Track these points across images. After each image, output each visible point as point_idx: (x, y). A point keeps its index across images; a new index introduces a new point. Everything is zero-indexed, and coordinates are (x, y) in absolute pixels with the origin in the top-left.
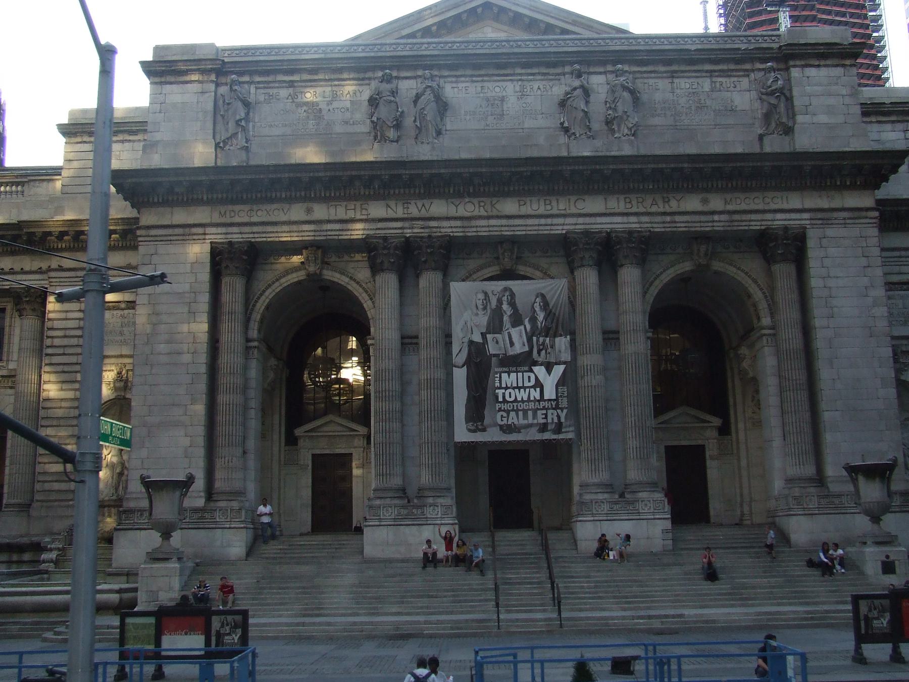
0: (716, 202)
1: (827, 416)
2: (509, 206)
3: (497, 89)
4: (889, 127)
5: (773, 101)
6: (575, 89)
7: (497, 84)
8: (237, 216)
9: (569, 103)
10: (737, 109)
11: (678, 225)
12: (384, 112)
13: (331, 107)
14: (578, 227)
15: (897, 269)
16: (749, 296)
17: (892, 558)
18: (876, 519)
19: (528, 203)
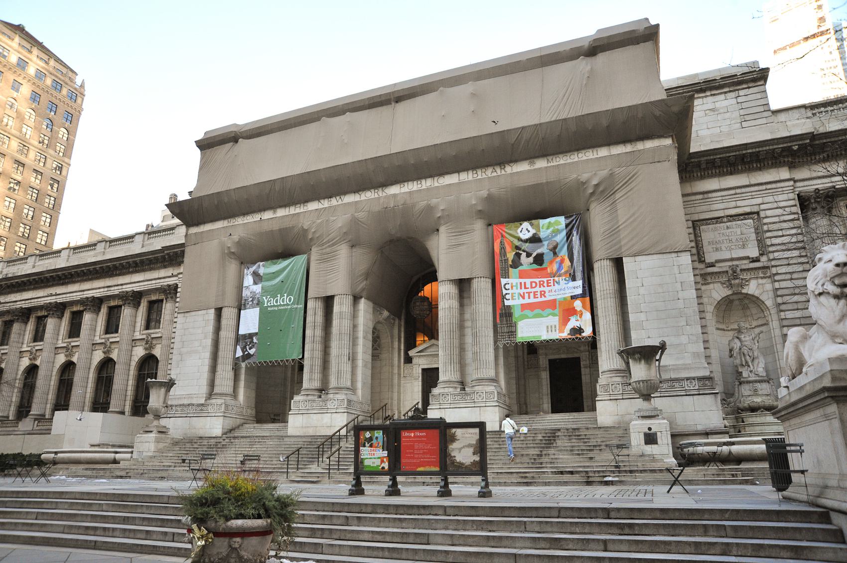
1: (632, 317)
4: (722, 97)
15: (733, 204)
17: (653, 431)
18: (647, 397)
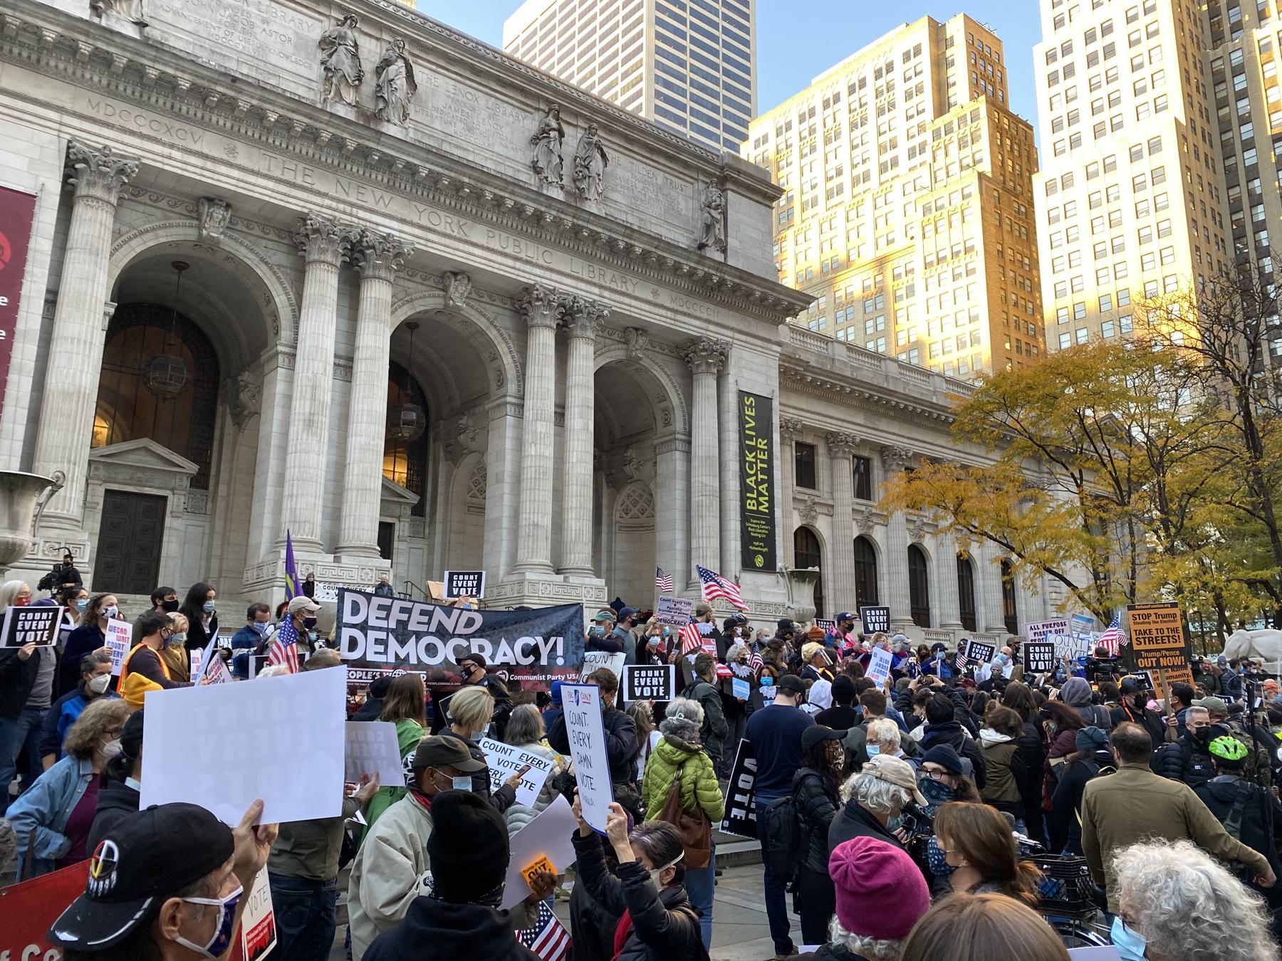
0: (665, 298)
2: (479, 234)
3: (469, 96)
5: (715, 214)
6: (554, 129)
7: (473, 91)
8: (117, 115)
9: (544, 142)
10: (683, 213)
11: (633, 309)
12: (342, 59)
13: (265, 26)
14: (544, 281)
16: (664, 398)
19: (497, 237)
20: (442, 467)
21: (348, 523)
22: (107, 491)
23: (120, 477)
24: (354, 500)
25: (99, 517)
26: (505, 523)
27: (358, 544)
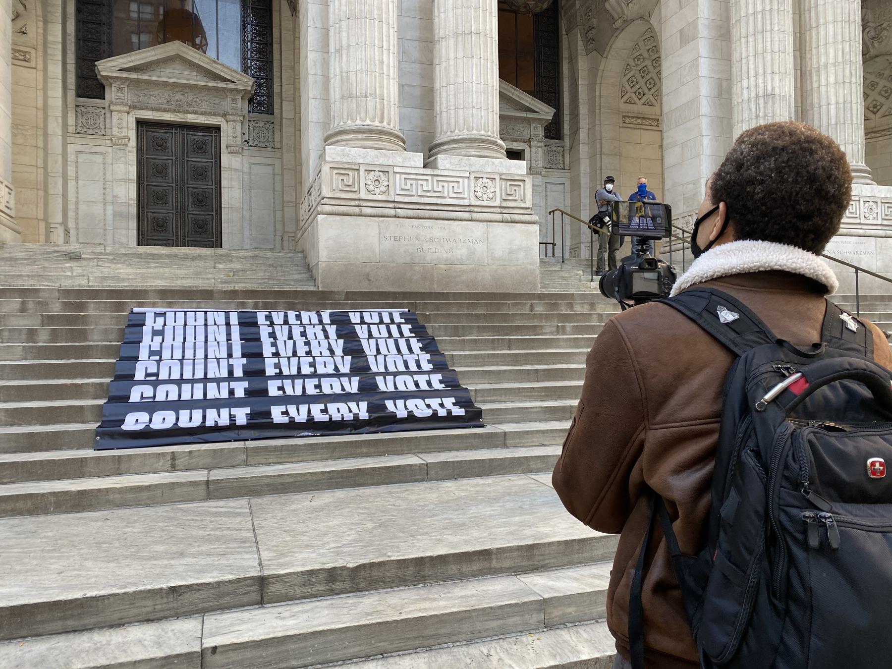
20: (583, 64)
21: (445, 99)
22: (141, 124)
23: (153, 101)
24: (452, 55)
25: (133, 157)
26: (705, 107)
27: (465, 134)
